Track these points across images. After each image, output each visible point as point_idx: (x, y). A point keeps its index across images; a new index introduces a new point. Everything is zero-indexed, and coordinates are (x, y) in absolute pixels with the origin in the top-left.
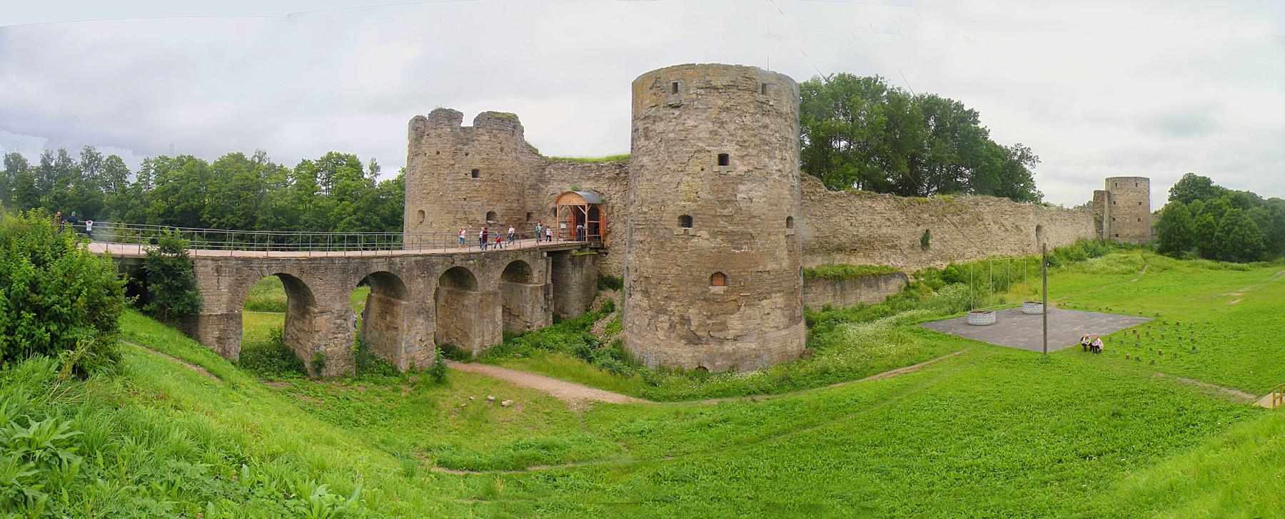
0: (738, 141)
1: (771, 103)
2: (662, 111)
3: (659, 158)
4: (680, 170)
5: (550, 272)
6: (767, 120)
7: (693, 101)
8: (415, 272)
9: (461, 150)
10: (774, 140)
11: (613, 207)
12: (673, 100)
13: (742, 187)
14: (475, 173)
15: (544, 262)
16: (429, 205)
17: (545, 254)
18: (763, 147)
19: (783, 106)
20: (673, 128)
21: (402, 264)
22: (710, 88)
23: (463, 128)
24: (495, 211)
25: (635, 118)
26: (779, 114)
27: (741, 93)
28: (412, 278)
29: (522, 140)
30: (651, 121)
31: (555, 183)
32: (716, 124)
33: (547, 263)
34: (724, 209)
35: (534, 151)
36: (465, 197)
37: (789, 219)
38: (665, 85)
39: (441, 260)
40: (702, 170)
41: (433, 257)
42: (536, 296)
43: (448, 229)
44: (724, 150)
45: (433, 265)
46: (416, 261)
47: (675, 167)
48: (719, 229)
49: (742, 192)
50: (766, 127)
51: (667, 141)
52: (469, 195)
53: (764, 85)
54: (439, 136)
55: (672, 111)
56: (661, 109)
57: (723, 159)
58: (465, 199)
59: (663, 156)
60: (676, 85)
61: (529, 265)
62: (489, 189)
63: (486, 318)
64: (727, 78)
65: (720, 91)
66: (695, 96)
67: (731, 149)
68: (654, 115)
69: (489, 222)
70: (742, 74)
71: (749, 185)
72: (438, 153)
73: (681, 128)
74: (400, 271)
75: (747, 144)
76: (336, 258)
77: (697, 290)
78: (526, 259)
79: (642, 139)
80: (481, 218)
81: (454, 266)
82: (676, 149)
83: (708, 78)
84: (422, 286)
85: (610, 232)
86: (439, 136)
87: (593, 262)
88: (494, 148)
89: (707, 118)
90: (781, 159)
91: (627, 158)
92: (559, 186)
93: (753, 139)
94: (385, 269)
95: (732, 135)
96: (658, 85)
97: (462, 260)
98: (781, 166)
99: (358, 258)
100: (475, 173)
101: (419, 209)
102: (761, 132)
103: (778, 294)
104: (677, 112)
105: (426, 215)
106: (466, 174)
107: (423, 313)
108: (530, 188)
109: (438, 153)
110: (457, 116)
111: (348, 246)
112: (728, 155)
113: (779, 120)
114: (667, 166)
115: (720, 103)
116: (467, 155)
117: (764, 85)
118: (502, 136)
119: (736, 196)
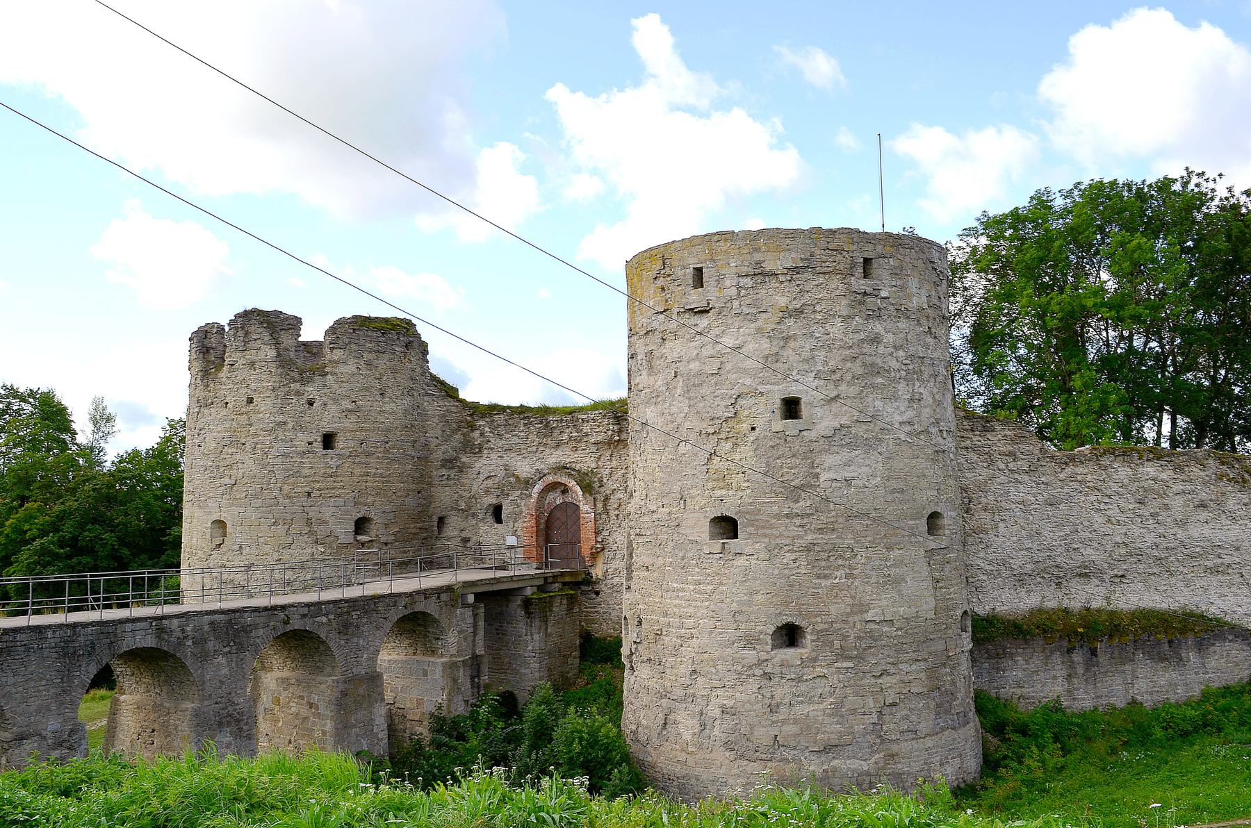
0: (819, 371)
1: (884, 294)
3: (674, 410)
4: (711, 430)
5: (481, 632)
6: (879, 328)
7: (731, 301)
8: (211, 645)
9: (298, 393)
10: (894, 364)
11: (607, 499)
12: (695, 298)
13: (830, 460)
14: (328, 441)
15: (468, 613)
16: (236, 510)
17: (471, 599)
18: (870, 380)
19: (909, 297)
20: (696, 352)
21: (183, 631)
22: (761, 274)
23: (305, 344)
24: (372, 515)
25: (632, 333)
26: (903, 313)
27: (821, 279)
28: (204, 657)
29: (425, 370)
30: (657, 337)
31: (493, 456)
32: (775, 343)
33: (475, 616)
34: (797, 501)
35: (450, 392)
36: (307, 489)
37: (934, 516)
39: (261, 620)
40: (753, 429)
41: (246, 615)
42: (455, 681)
43: (276, 556)
44: (793, 390)
45: (246, 630)
46: (211, 624)
48: (787, 541)
49: (830, 468)
50: (876, 339)
52: (317, 485)
53: (867, 261)
54: (252, 364)
55: (695, 319)
57: (791, 408)
58: (309, 494)
60: (699, 271)
61: (437, 621)
62: (357, 471)
63: (354, 726)
64: (794, 255)
65: (782, 278)
66: (734, 291)
67: (806, 389)
69: (359, 538)
70: (823, 244)
71: (845, 454)
72: (250, 401)
73: (712, 352)
74: (180, 643)
75: (837, 377)
76: (50, 626)
77: (751, 656)
78: (431, 607)
79: (644, 373)
80: (344, 531)
81: (289, 628)
83: (758, 257)
84: (225, 671)
85: (603, 549)
86: (252, 364)
87: (570, 609)
88: (367, 389)
89: (759, 331)
90: (912, 400)
91: (623, 402)
92: (501, 462)
93: (849, 365)
94: (150, 642)
95: (807, 361)
97: (304, 616)
98: (909, 415)
99: (92, 624)
100: (328, 441)
101: (215, 517)
102: (865, 351)
103: (914, 667)
104: (703, 322)
105: (229, 530)
106: (310, 444)
107: (229, 724)
108: (443, 466)
109: (250, 401)
110: (294, 323)
111: (70, 601)
112: (799, 399)
113: (903, 324)
114: (687, 424)
115: (782, 301)
116: (311, 403)
117: (867, 261)
118: (383, 363)
119: (817, 476)
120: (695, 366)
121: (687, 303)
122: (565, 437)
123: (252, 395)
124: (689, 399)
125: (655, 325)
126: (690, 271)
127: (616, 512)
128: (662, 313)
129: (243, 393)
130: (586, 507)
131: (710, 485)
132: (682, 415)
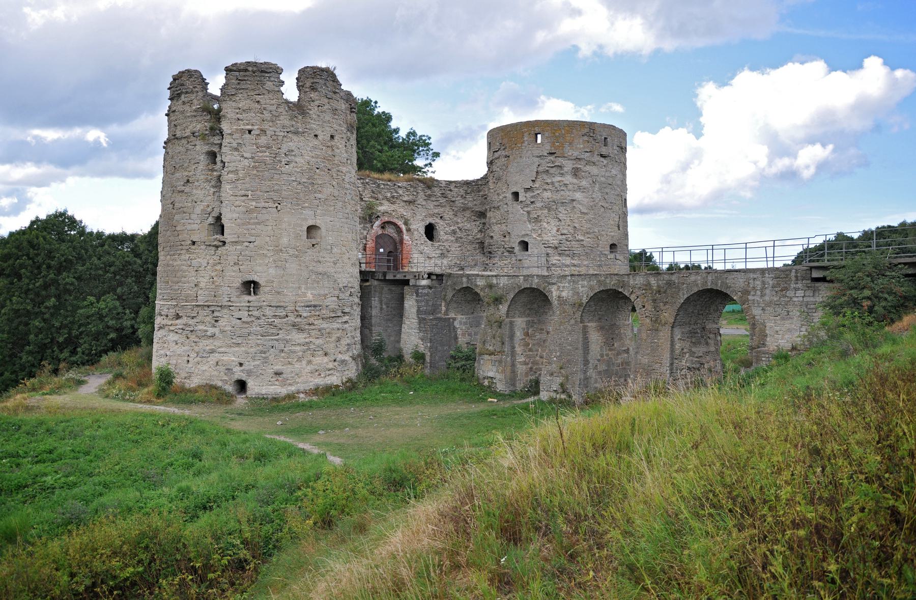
2: (597, 158)
3: (594, 196)
12: (604, 151)
30: (583, 163)
38: (599, 137)
47: (607, 205)
55: (602, 159)
56: (595, 155)
59: (597, 195)
68: (588, 159)
72: (332, 137)
73: (609, 175)
82: (606, 190)
96: (592, 135)
114: (600, 204)
120: (603, 179)
122: (389, 195)
123: (335, 133)
124: (602, 193)
125: (582, 156)
127: (416, 242)
129: (329, 132)
130: (407, 237)
131: (610, 230)
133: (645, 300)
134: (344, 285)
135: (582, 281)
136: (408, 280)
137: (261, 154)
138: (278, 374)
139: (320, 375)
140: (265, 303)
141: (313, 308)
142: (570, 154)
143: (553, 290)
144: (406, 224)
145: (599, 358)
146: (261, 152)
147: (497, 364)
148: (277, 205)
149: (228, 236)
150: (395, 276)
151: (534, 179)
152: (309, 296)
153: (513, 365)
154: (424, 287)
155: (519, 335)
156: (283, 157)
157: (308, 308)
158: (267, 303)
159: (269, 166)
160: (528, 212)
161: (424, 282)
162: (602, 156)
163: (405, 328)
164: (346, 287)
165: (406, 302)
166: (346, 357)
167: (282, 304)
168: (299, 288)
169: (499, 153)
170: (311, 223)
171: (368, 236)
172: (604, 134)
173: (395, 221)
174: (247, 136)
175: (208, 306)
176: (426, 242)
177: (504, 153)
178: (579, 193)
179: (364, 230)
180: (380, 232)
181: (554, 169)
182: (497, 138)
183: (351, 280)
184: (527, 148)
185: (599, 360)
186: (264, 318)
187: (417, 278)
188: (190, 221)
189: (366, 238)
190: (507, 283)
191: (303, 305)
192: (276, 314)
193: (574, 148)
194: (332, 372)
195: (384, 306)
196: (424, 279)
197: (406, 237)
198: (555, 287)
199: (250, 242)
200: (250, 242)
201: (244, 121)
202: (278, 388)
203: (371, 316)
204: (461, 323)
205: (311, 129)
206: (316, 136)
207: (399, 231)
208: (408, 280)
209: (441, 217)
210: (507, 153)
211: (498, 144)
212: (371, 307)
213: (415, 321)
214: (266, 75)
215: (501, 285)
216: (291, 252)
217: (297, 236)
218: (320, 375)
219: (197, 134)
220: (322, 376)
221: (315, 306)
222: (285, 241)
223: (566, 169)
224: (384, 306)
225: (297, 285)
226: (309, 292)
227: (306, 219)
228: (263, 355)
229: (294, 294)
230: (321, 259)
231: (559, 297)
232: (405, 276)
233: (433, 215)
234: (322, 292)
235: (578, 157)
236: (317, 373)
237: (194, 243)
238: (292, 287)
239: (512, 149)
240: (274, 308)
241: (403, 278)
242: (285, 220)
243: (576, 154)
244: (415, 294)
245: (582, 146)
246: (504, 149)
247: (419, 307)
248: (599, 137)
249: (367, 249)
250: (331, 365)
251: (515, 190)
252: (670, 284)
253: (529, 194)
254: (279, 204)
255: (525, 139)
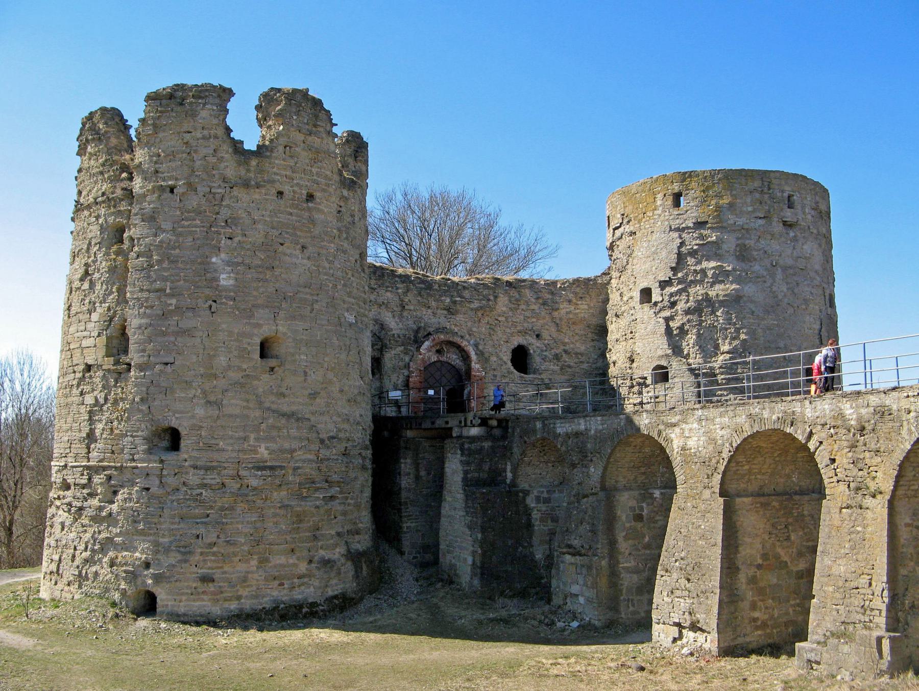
3: (774, 289)
12: (788, 215)
38: (779, 194)
51: (785, 269)
56: (774, 224)
72: (310, 197)
109: (310, 197)
120: (790, 262)
121: (784, 217)
124: (787, 283)
126: (786, 195)
128: (760, 218)
130: (477, 366)
132: (783, 294)
133: (836, 447)
134: (331, 434)
135: (721, 417)
136: (451, 429)
137: (186, 223)
138: (206, 579)
139: (282, 584)
140: (187, 464)
141: (268, 473)
142: (731, 222)
143: (673, 436)
144: (476, 346)
145: (760, 561)
146: (187, 219)
147: (584, 571)
148: (210, 302)
149: (134, 356)
150: (433, 423)
151: (674, 265)
152: (263, 452)
153: (614, 574)
154: (473, 439)
155: (624, 518)
156: (223, 227)
157: (260, 473)
158: (192, 463)
159: (198, 242)
160: (667, 320)
161: (475, 431)
162: (785, 223)
163: (446, 509)
164: (333, 438)
165: (447, 465)
166: (337, 553)
167: (214, 464)
168: (245, 439)
169: (621, 230)
170: (266, 331)
171: (411, 364)
172: (787, 188)
173: (457, 340)
174: (167, 195)
175: (104, 468)
176: (512, 373)
177: (627, 228)
178: (750, 284)
179: (406, 353)
180: (434, 358)
181: (706, 248)
182: (617, 206)
183: (346, 426)
184: (662, 218)
185: (759, 567)
186: (185, 489)
187: (463, 424)
188: (85, 334)
189: (407, 366)
190: (601, 427)
191: (250, 466)
192: (205, 481)
193: (738, 212)
194: (306, 580)
195: (423, 473)
196: (474, 426)
197: (475, 366)
198: (677, 430)
199: (167, 364)
200: (167, 364)
201: (165, 174)
202: (204, 606)
203: (400, 488)
204: (538, 499)
205: (273, 182)
206: (280, 193)
207: (466, 357)
208: (451, 429)
209: (538, 336)
210: (632, 228)
211: (619, 216)
212: (400, 474)
213: (460, 496)
214: (200, 101)
215: (593, 432)
216: (234, 375)
217: (243, 354)
218: (282, 584)
219: (100, 199)
220: (286, 586)
221: (272, 468)
222: (222, 360)
223: (725, 247)
224: (423, 473)
225: (241, 434)
226: (263, 446)
227: (258, 326)
228: (182, 549)
229: (237, 448)
230: (283, 390)
231: (683, 449)
232: (447, 423)
233: (524, 332)
234: (287, 445)
235: (746, 227)
236: (277, 582)
237: (88, 368)
238: (231, 438)
239: (639, 222)
240: (202, 472)
241: (444, 426)
242: (224, 326)
243: (740, 222)
244: (459, 452)
245: (750, 209)
246: (629, 222)
247: (466, 473)
248: (779, 194)
249: (411, 385)
250: (303, 567)
251: (644, 285)
252: (882, 413)
253: (669, 290)
254: (215, 301)
255: (659, 203)
